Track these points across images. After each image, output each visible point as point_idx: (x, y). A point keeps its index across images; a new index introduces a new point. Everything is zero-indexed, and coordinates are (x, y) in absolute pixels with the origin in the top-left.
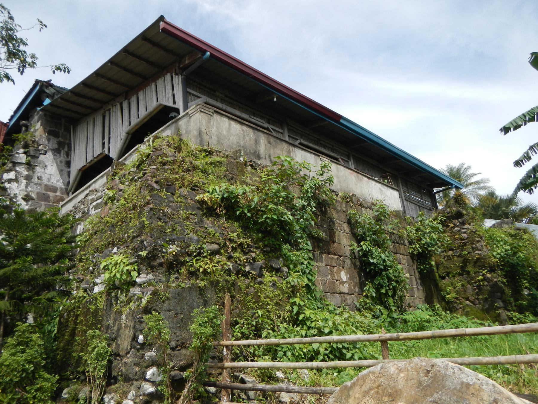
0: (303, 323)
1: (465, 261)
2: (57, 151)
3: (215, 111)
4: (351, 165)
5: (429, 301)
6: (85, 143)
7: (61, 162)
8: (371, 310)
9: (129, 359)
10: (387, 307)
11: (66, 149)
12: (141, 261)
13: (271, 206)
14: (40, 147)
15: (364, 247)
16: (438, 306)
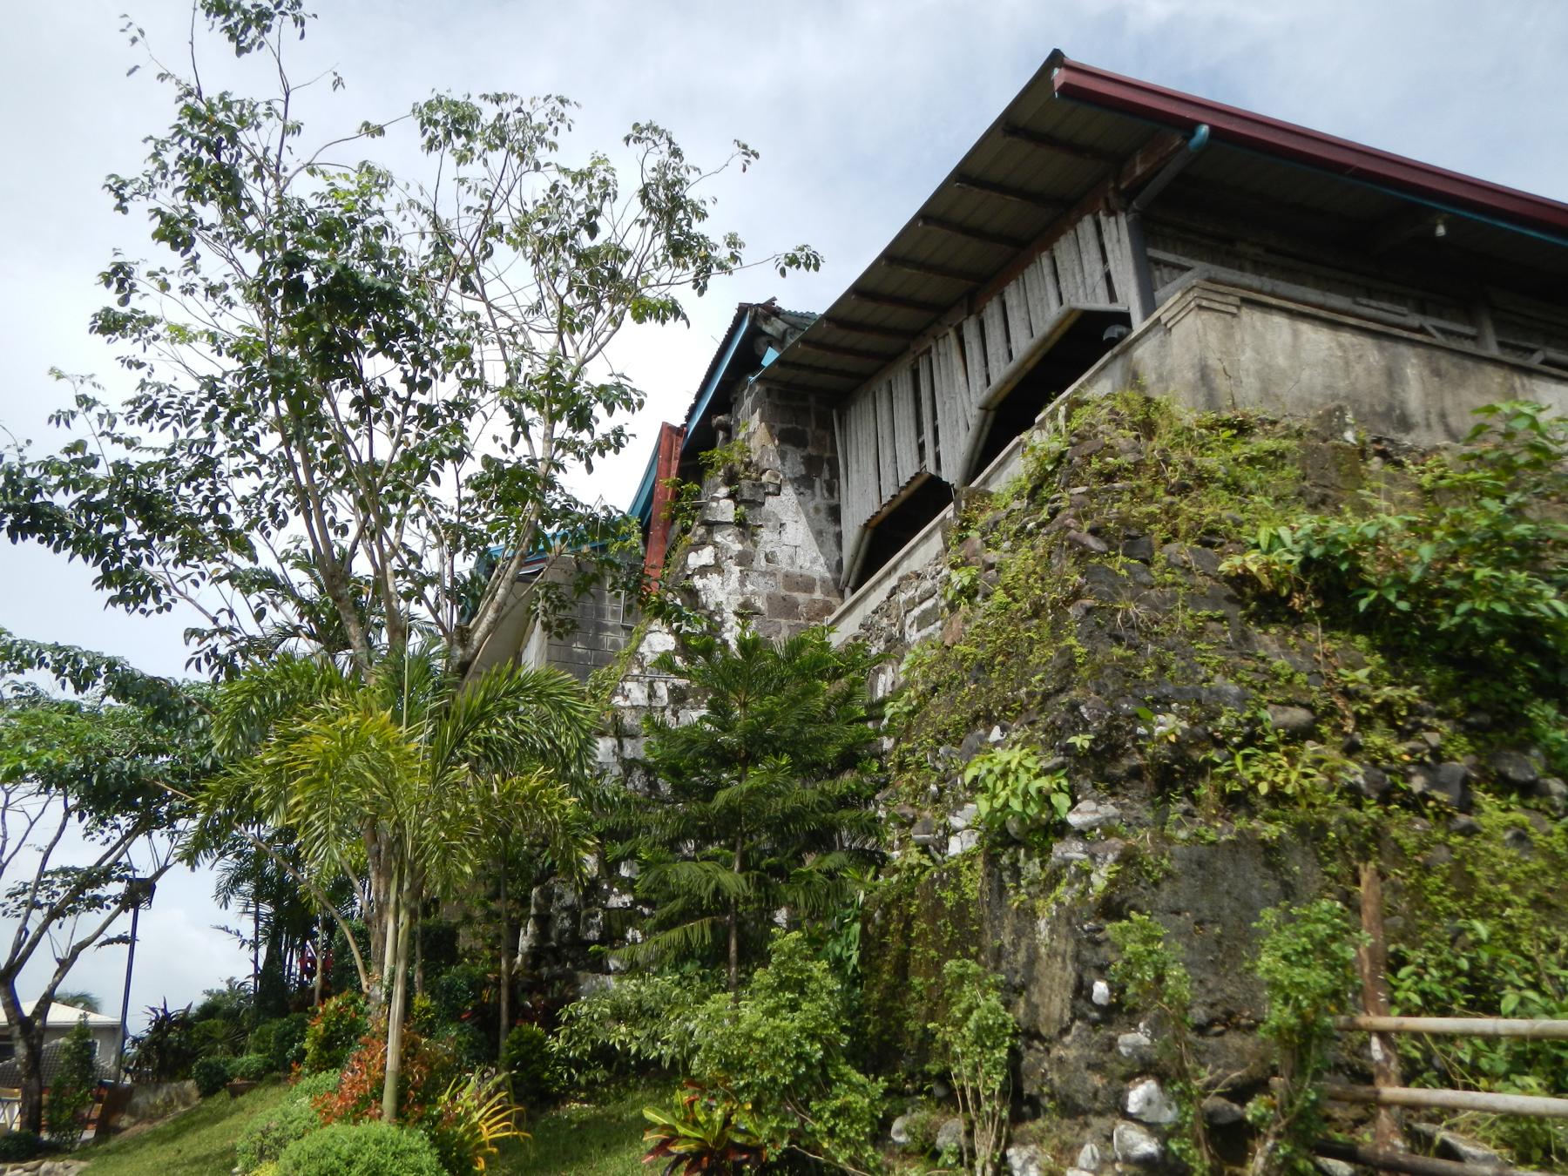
2: (803, 483)
3: (1247, 302)
6: (873, 451)
7: (817, 510)
9: (1070, 1050)
11: (826, 475)
14: (765, 478)
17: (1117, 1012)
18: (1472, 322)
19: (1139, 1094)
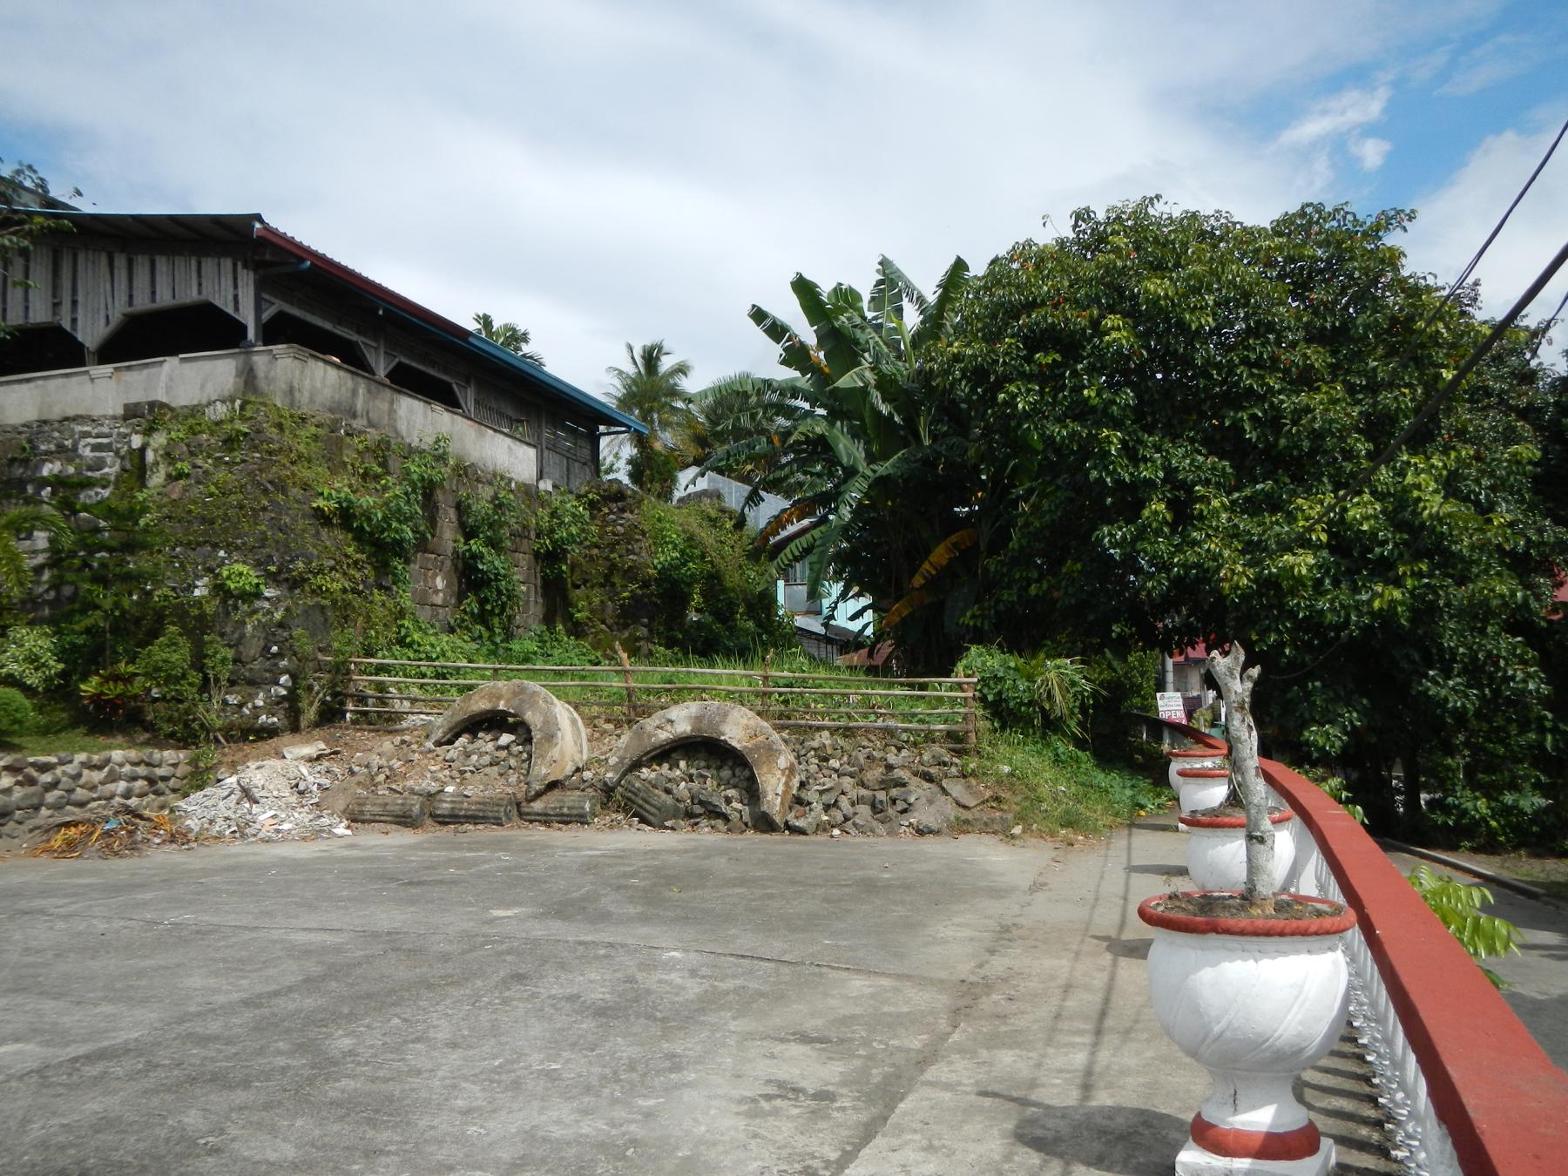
0: (410, 646)
1: (613, 567)
4: (468, 397)
5: (548, 620)
8: (467, 628)
9: (256, 666)
10: (490, 629)
12: (269, 575)
13: (394, 525)
15: (474, 548)
16: (560, 627)
17: (280, 655)
18: (376, 340)
19: (284, 679)
